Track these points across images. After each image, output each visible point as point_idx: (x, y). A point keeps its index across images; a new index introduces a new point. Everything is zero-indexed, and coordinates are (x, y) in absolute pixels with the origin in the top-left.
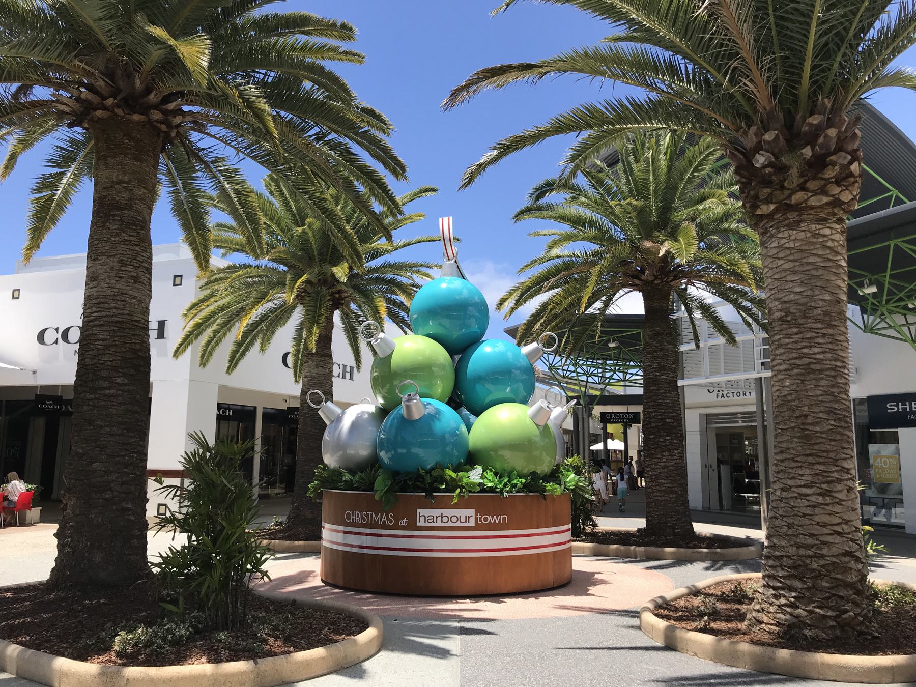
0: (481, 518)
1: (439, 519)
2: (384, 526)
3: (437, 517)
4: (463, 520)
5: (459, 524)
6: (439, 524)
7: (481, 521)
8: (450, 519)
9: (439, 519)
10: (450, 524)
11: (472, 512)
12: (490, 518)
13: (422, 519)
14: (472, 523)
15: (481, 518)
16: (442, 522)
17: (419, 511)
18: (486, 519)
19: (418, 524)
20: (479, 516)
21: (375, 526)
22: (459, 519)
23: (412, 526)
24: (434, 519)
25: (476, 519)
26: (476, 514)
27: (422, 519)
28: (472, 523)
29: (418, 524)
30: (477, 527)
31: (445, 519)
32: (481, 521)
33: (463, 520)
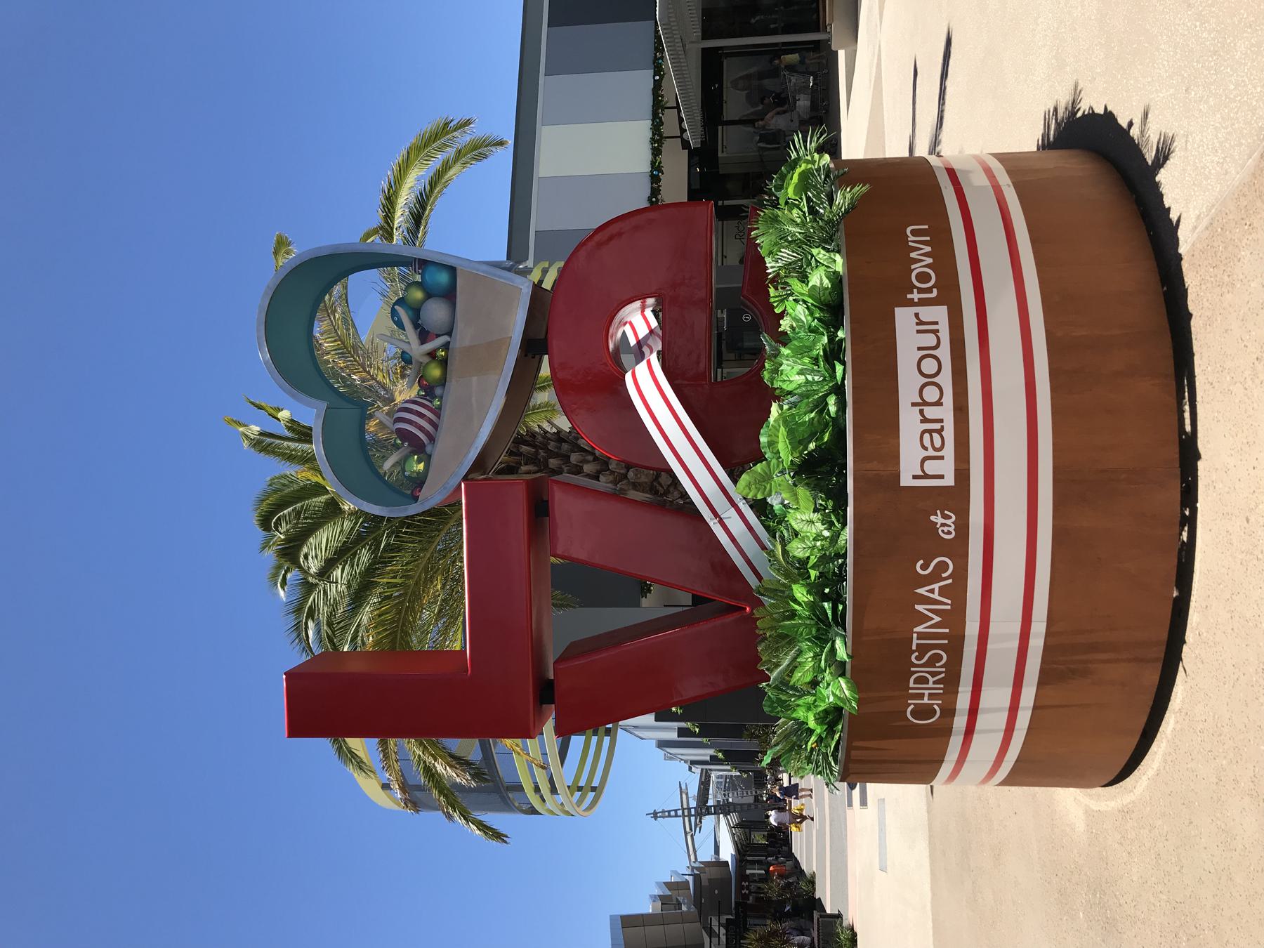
0: (921, 291)
1: (930, 412)
2: (957, 591)
3: (925, 420)
4: (930, 340)
5: (944, 353)
6: (946, 412)
7: (929, 290)
8: (930, 380)
9: (930, 412)
10: (946, 379)
11: (904, 318)
12: (917, 269)
13: (931, 467)
14: (940, 314)
15: (921, 291)
16: (939, 403)
17: (906, 480)
18: (923, 277)
19: (949, 481)
20: (915, 296)
21: (955, 617)
22: (927, 353)
23: (956, 498)
24: (932, 430)
25: (922, 303)
26: (911, 303)
27: (931, 467)
28: (940, 314)
29: (949, 481)
30: (948, 295)
31: (931, 394)
32: (929, 290)
33: (930, 340)
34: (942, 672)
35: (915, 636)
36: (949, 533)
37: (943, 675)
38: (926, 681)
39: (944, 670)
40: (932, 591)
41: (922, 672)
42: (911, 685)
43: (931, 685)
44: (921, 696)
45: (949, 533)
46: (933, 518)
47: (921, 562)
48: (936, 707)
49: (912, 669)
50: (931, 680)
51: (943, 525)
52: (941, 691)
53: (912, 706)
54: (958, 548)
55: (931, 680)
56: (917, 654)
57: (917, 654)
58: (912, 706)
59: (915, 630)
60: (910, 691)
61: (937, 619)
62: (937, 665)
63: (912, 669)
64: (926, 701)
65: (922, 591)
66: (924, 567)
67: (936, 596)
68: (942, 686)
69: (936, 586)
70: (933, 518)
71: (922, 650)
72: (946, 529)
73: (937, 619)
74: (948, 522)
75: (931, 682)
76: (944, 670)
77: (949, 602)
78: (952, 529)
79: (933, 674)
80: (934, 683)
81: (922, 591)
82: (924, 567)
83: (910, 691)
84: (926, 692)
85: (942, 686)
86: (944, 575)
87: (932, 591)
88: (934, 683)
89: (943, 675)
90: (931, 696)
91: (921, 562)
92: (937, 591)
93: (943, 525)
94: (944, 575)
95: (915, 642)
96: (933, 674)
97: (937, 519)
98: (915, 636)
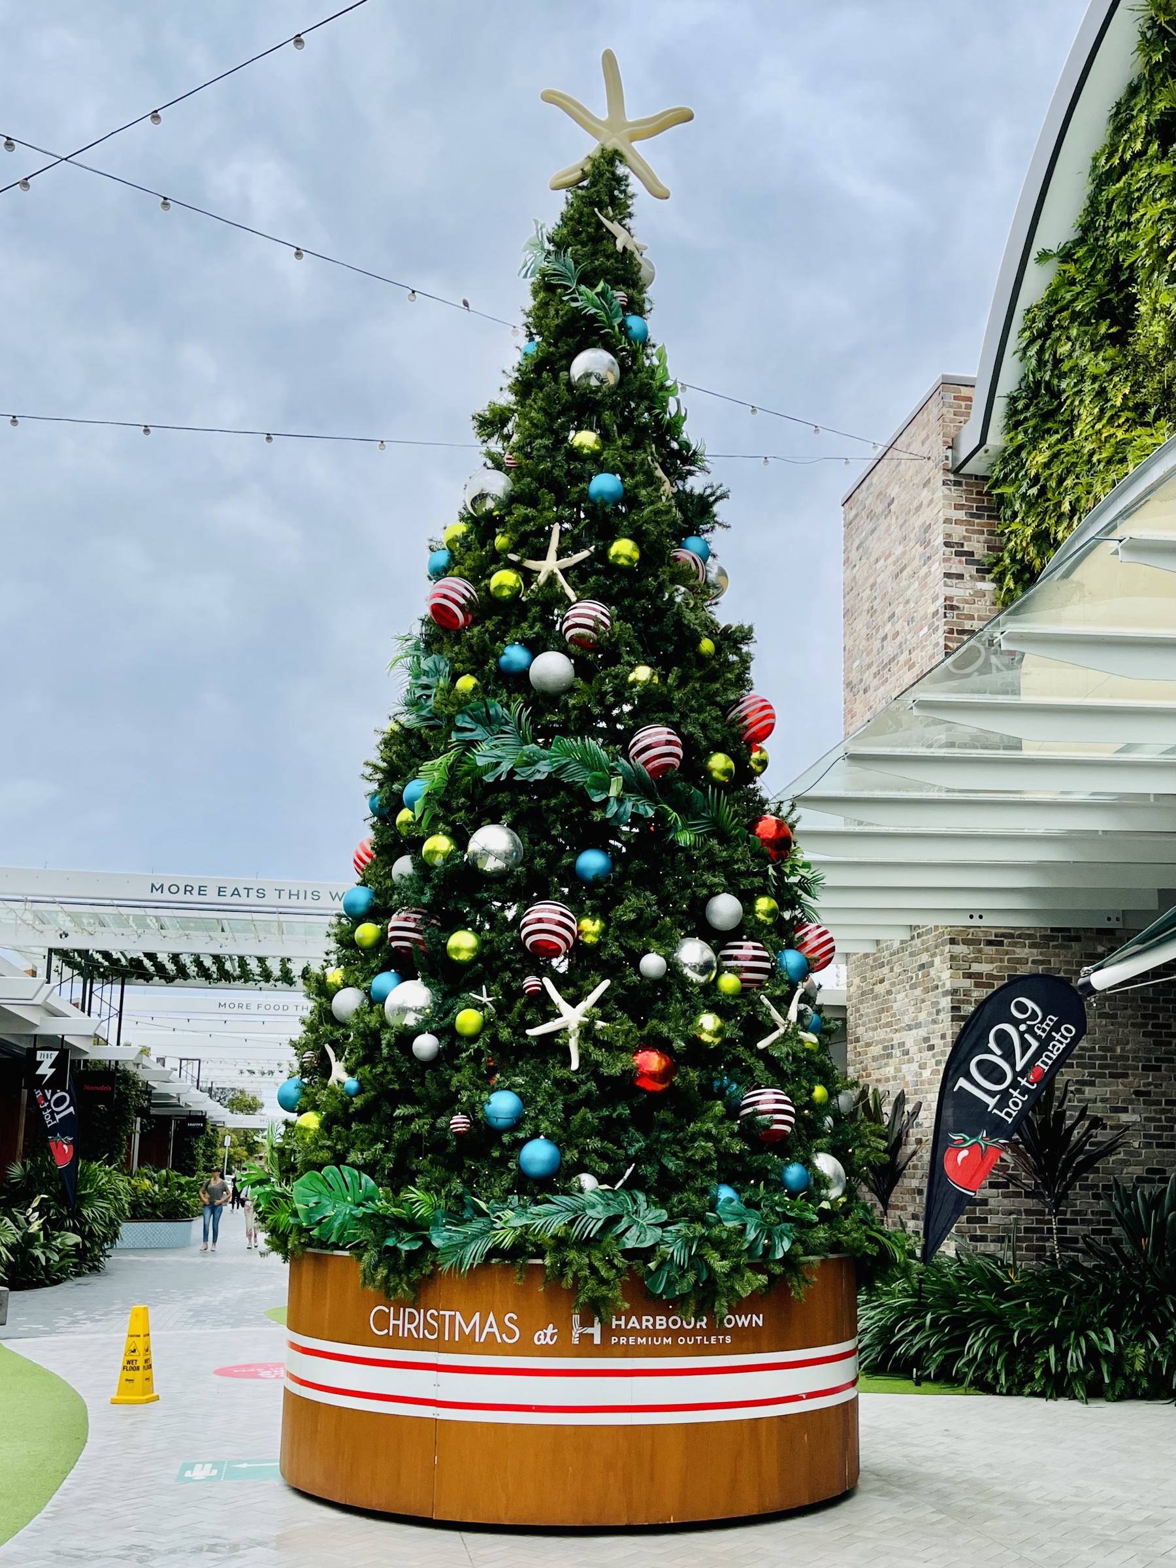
2: (490, 1347)
21: (466, 1345)
34: (419, 1335)
35: (453, 1313)
36: (539, 1340)
37: (416, 1336)
38: (411, 1322)
39: (421, 1336)
40: (491, 1326)
41: (419, 1318)
42: (408, 1310)
43: (407, 1326)
44: (396, 1318)
45: (539, 1340)
46: (551, 1326)
47: (515, 1317)
48: (386, 1331)
49: (422, 1311)
50: (412, 1327)
51: (545, 1334)
52: (401, 1335)
53: (387, 1311)
54: (525, 1348)
55: (412, 1327)
56: (436, 1314)
57: (436, 1314)
58: (387, 1311)
59: (458, 1313)
60: (402, 1309)
61: (467, 1331)
62: (426, 1331)
63: (422, 1311)
64: (392, 1322)
65: (491, 1318)
66: (510, 1319)
67: (487, 1329)
68: (406, 1335)
69: (495, 1330)
70: (551, 1326)
71: (439, 1319)
72: (542, 1337)
73: (467, 1331)
74: (548, 1339)
75: (410, 1326)
76: (421, 1336)
77: (482, 1340)
78: (542, 1342)
79: (417, 1329)
80: (409, 1329)
81: (491, 1318)
82: (510, 1319)
83: (402, 1309)
84: (400, 1323)
85: (406, 1335)
86: (504, 1336)
87: (491, 1326)
88: (409, 1329)
89: (416, 1336)
90: (396, 1327)
91: (515, 1318)
92: (491, 1330)
93: (545, 1334)
94: (504, 1336)
95: (447, 1313)
96: (417, 1329)
97: (550, 1330)
98: (453, 1313)
